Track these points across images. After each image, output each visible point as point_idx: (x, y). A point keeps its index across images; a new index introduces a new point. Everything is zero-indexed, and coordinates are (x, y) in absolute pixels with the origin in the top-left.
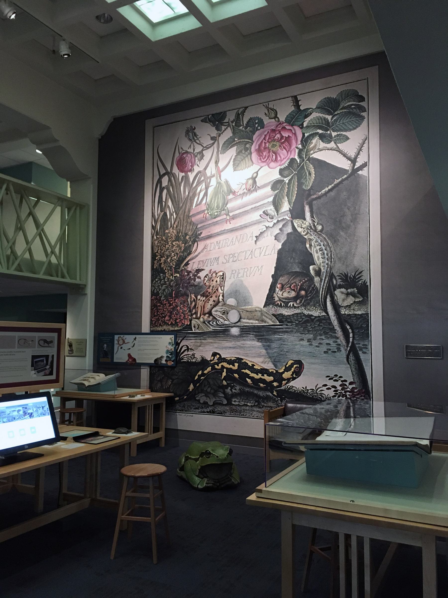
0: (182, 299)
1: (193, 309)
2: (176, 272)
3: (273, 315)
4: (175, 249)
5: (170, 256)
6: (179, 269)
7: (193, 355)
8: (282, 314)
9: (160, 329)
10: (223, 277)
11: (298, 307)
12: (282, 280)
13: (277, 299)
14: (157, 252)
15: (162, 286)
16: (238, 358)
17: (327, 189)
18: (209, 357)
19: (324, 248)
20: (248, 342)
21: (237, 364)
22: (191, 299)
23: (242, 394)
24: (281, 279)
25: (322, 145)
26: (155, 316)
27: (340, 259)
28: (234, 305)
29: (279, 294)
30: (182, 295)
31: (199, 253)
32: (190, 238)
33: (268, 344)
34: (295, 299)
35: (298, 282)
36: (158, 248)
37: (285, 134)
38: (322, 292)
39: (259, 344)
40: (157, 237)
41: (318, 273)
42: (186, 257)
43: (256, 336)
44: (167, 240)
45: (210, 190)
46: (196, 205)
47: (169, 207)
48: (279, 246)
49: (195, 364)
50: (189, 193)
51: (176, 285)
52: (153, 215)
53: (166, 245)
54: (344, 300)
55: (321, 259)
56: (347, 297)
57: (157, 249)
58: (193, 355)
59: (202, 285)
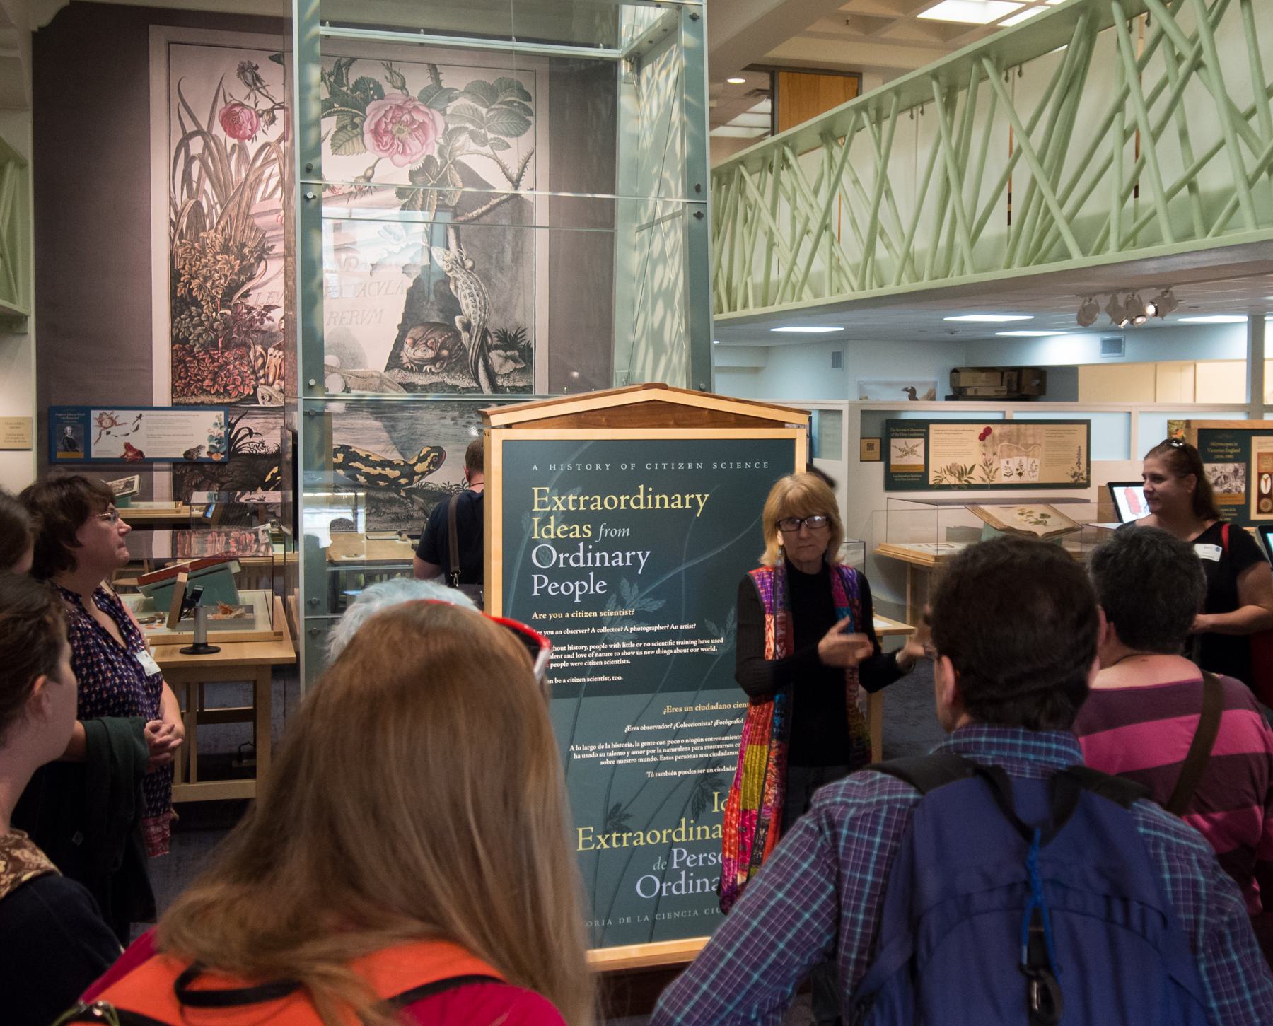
0: (237, 352)
1: (259, 369)
2: (224, 306)
3: (400, 383)
4: (220, 268)
5: (210, 277)
6: (230, 302)
7: (260, 443)
8: (414, 383)
9: (192, 400)
11: (438, 373)
12: (415, 332)
13: (405, 360)
14: (183, 268)
15: (194, 329)
16: (343, 447)
17: (479, 211)
19: (475, 293)
20: (360, 422)
21: (342, 455)
22: (255, 353)
24: (411, 331)
25: (473, 146)
26: (181, 378)
27: (497, 311)
28: (334, 365)
30: (239, 346)
31: (270, 280)
32: (251, 252)
33: (392, 423)
34: (433, 361)
35: (438, 338)
36: (185, 261)
38: (471, 354)
39: (378, 424)
40: (181, 242)
41: (467, 326)
42: (243, 284)
43: (372, 413)
44: (204, 250)
46: (263, 199)
47: (205, 192)
49: (266, 456)
50: (247, 176)
51: (224, 329)
52: (172, 203)
53: (201, 258)
54: (501, 366)
55: (471, 308)
56: (506, 361)
57: (182, 263)
58: (262, 443)
59: (277, 332)
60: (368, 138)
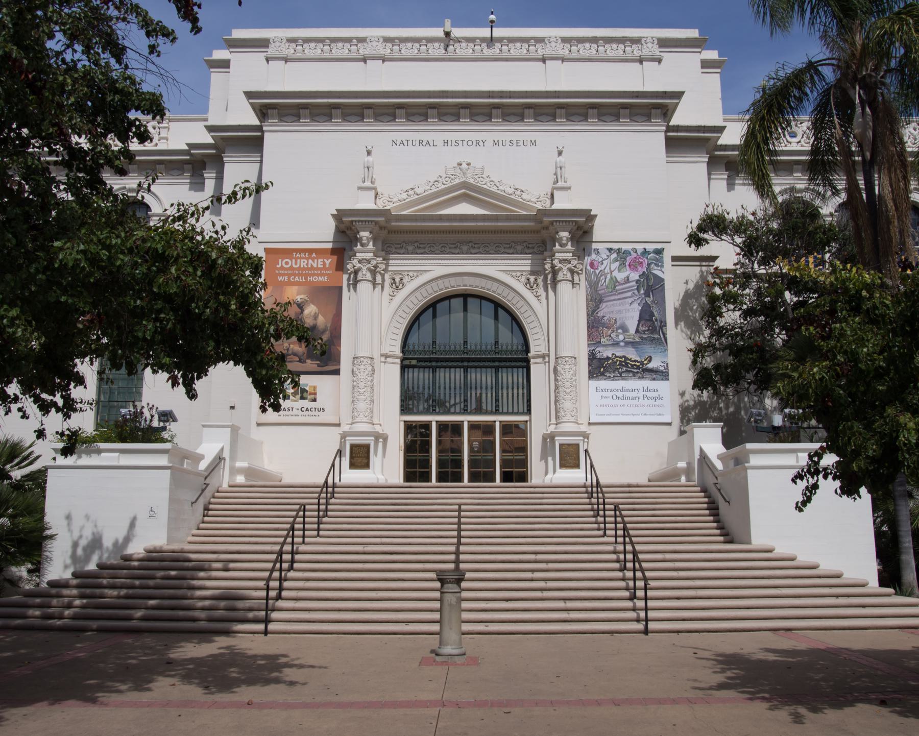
10: (616, 320)
12: (642, 322)
18: (610, 356)
23: (627, 371)
25: (655, 268)
29: (641, 328)
34: (648, 330)
37: (641, 260)
38: (658, 328)
45: (607, 280)
48: (640, 308)
60: (628, 267)
